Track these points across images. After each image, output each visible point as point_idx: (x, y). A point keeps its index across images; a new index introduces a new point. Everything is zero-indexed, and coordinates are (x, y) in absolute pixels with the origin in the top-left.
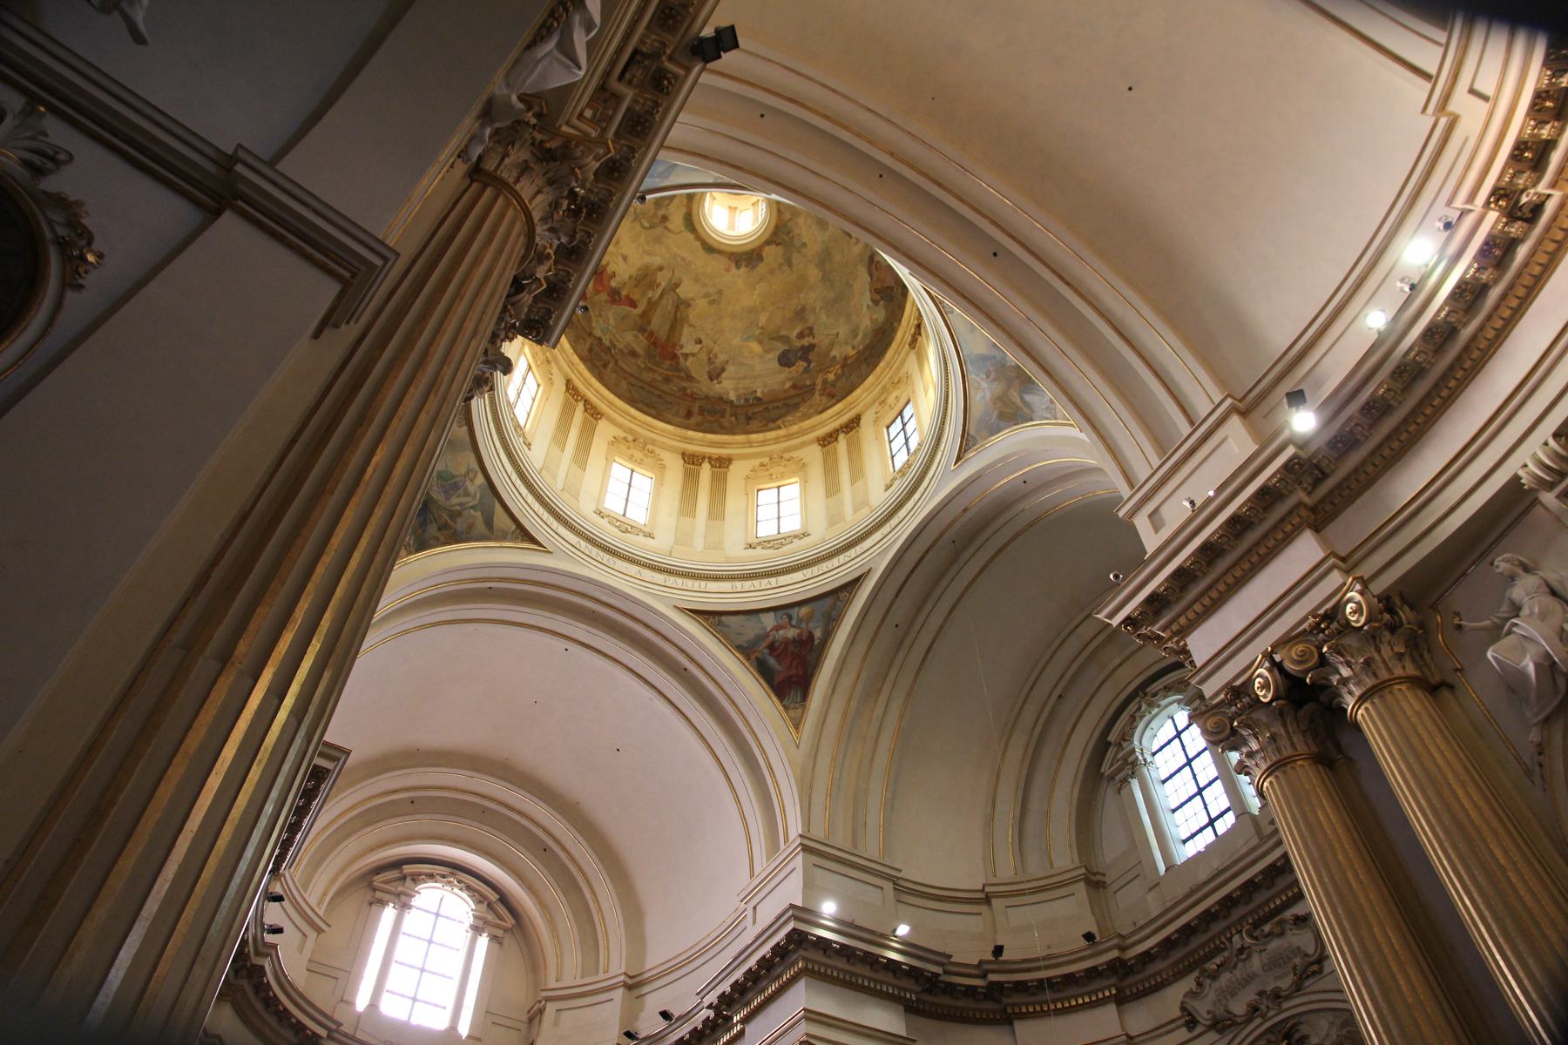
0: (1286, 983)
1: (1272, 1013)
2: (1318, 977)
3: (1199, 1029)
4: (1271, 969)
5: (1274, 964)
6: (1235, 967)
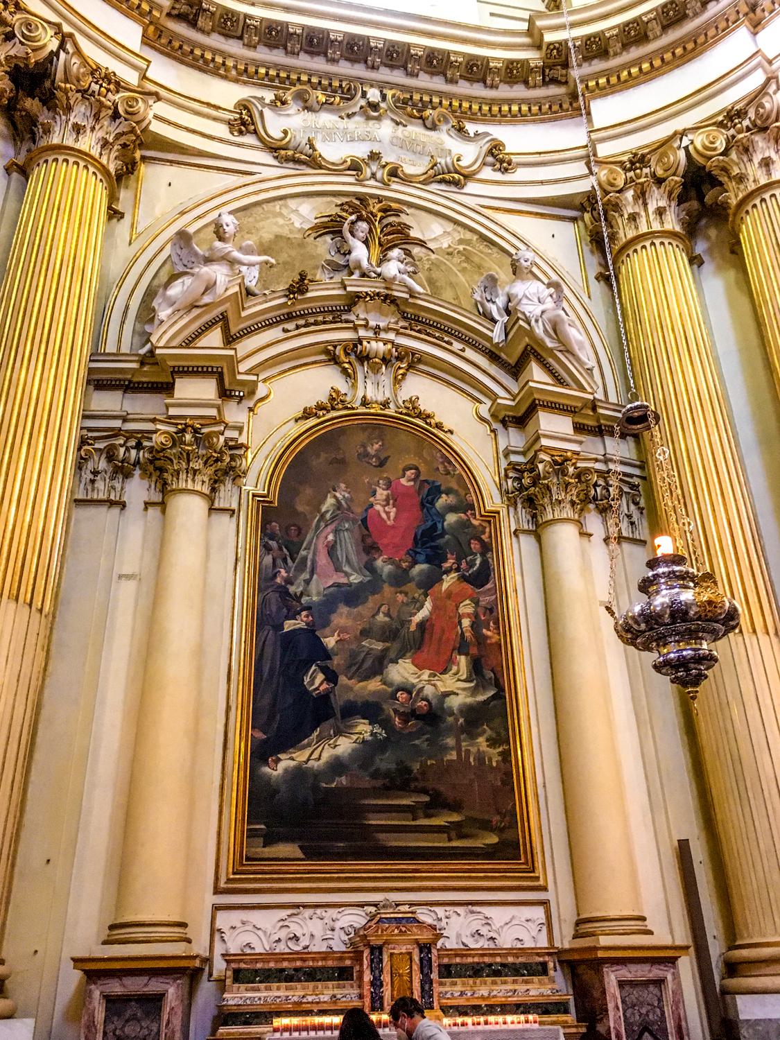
0: (414, 167)
1: (372, 182)
2: (453, 189)
3: (250, 139)
4: (402, 147)
5: (403, 144)
6: (349, 116)
